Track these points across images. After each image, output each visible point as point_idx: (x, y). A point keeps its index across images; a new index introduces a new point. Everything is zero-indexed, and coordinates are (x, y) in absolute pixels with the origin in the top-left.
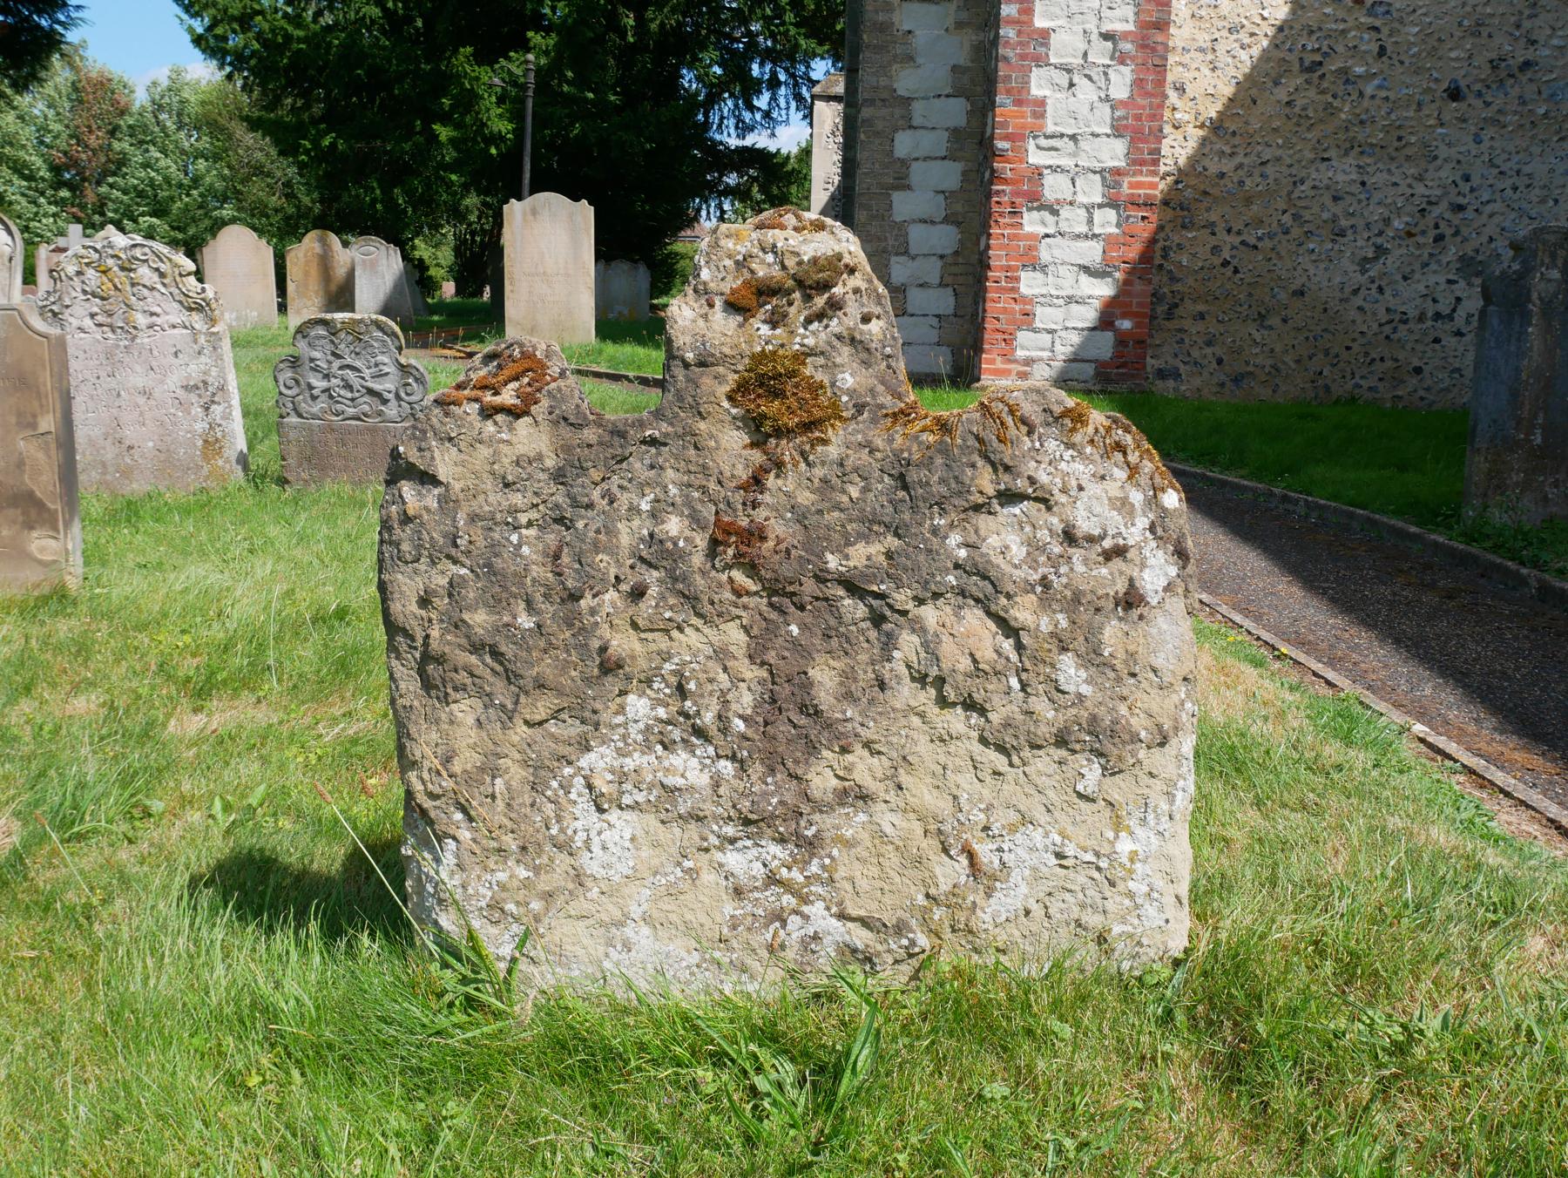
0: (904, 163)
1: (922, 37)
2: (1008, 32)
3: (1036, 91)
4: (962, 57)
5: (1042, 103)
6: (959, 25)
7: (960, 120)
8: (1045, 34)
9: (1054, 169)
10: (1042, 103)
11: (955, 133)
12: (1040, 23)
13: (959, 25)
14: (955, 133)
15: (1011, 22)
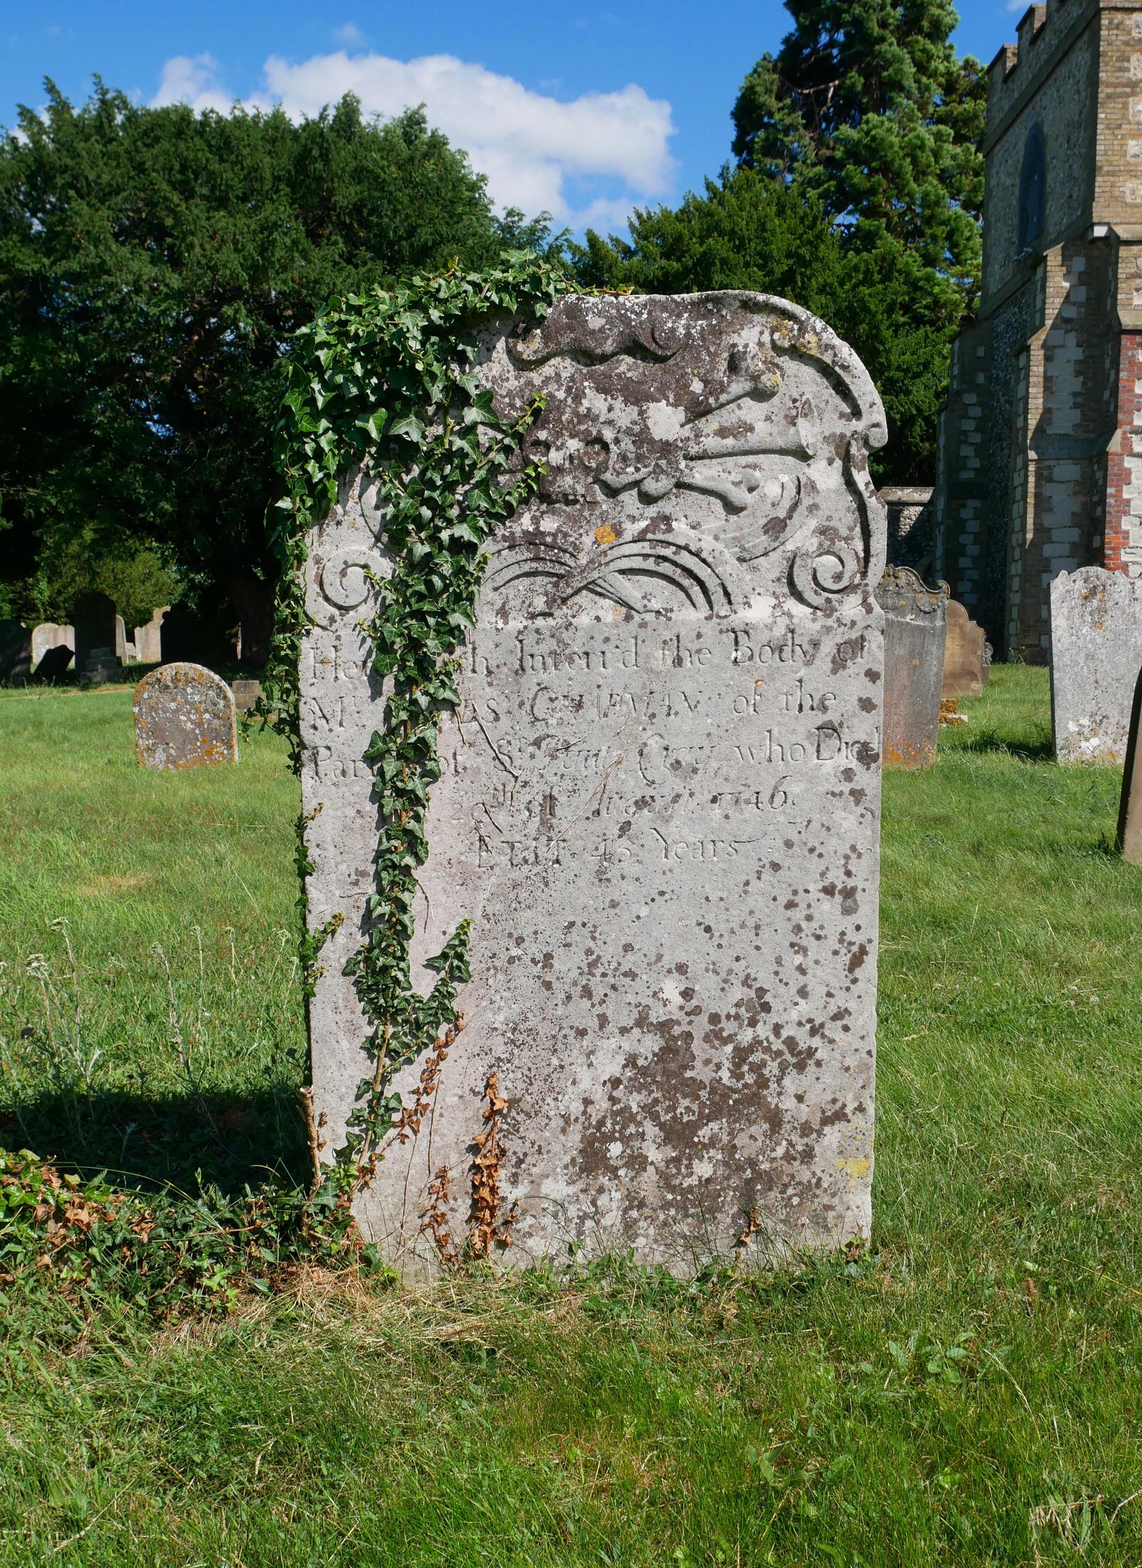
0: (1048, 560)
1: (1056, 499)
2: (1110, 501)
3: (1124, 527)
4: (1077, 508)
5: (1127, 532)
6: (1075, 493)
7: (1077, 539)
8: (1128, 501)
9: (1134, 563)
10: (1127, 532)
11: (1074, 545)
12: (1125, 496)
13: (1075, 493)
14: (1074, 545)
15: (1112, 496)
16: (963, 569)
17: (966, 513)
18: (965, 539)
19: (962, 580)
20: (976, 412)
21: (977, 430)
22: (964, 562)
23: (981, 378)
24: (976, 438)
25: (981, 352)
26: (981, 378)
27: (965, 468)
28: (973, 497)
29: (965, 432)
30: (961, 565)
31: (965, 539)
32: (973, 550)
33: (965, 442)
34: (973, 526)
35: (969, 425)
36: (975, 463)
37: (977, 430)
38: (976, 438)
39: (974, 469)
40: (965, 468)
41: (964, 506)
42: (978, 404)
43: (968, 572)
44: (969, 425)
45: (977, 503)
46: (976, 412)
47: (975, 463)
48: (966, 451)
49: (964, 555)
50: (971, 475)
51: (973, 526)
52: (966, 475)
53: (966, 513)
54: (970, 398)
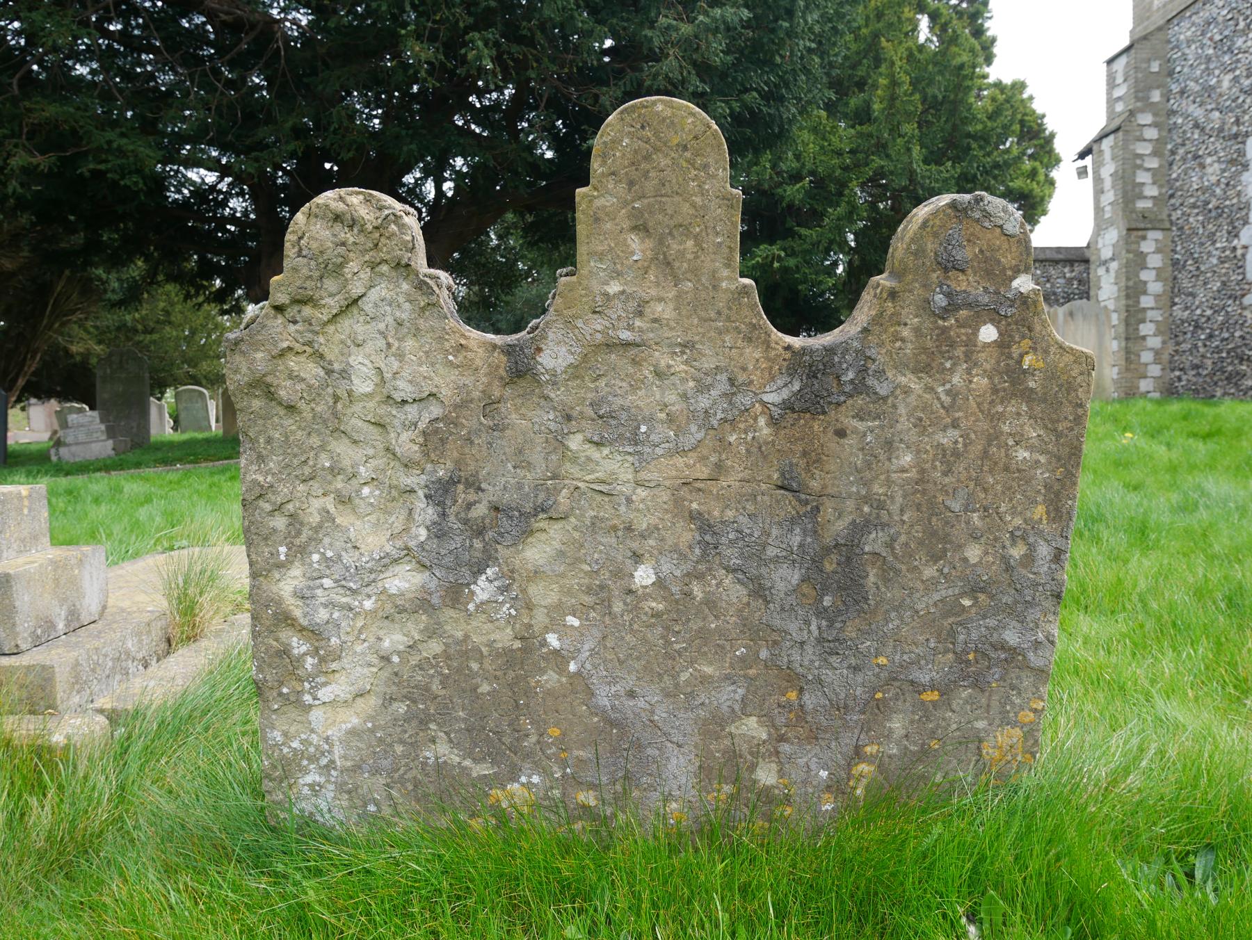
16: (1145, 309)
17: (1147, 247)
18: (1145, 276)
19: (1143, 321)
20: (1152, 133)
21: (1155, 153)
22: (1146, 301)
23: (1156, 96)
24: (1153, 163)
25: (1155, 67)
26: (1156, 96)
27: (1142, 197)
28: (1153, 229)
29: (1141, 156)
30: (1143, 305)
31: (1145, 276)
32: (1155, 287)
33: (1140, 167)
34: (1155, 261)
35: (1144, 149)
36: (1151, 191)
37: (1155, 153)
38: (1153, 163)
39: (1153, 198)
40: (1142, 197)
41: (1144, 238)
42: (1155, 125)
43: (1150, 314)
44: (1144, 149)
45: (1158, 235)
46: (1152, 133)
47: (1151, 191)
48: (1143, 177)
49: (1145, 293)
50: (1149, 204)
51: (1155, 261)
52: (1141, 205)
53: (1147, 247)
54: (1145, 118)
